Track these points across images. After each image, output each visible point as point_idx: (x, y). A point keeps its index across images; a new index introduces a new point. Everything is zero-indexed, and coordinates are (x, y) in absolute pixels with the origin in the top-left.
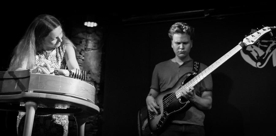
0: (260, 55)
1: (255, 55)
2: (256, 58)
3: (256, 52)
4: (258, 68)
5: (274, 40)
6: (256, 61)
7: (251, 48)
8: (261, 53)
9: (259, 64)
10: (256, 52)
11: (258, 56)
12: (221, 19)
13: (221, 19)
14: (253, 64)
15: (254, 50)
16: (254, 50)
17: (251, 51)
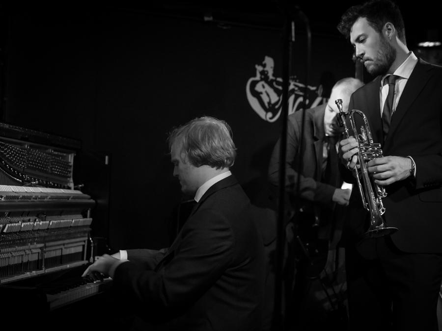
0: (273, 102)
1: (266, 100)
2: (266, 105)
3: (268, 95)
4: (267, 122)
5: (293, 81)
6: (267, 110)
7: (261, 87)
8: (274, 98)
9: (270, 115)
10: (268, 95)
11: (269, 103)
12: (225, 28)
13: (225, 28)
14: (262, 113)
15: (266, 92)
16: (266, 92)
17: (261, 93)
